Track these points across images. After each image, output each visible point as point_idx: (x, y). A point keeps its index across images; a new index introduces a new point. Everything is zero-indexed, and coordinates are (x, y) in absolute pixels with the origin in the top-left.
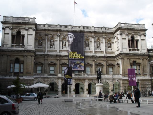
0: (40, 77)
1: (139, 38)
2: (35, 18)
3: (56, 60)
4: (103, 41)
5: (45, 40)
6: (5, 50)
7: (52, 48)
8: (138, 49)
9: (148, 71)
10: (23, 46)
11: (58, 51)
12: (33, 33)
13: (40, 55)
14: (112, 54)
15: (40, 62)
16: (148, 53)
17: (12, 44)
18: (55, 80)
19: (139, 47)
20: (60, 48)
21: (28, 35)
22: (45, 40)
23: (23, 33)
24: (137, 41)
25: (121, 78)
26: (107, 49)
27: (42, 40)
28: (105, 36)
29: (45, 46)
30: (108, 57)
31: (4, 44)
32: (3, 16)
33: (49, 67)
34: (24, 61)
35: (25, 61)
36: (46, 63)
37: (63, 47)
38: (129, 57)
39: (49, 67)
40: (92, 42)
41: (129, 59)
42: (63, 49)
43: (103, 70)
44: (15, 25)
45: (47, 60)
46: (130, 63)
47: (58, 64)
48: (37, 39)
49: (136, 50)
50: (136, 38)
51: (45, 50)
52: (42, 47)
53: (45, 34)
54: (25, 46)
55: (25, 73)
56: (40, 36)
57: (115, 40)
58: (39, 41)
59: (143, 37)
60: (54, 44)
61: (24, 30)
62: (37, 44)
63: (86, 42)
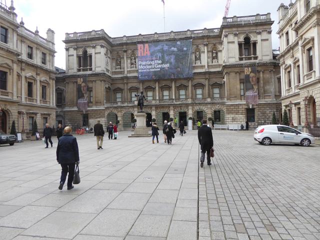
1: (258, 38)
2: (102, 30)
4: (204, 49)
6: (70, 76)
7: (133, 67)
9: (272, 90)
10: (91, 69)
12: (103, 51)
15: (118, 88)
18: (130, 109)
19: (258, 53)
21: (95, 53)
24: (255, 44)
27: (121, 58)
28: (208, 42)
30: (210, 73)
32: (66, 34)
34: (92, 88)
36: (126, 88)
38: (239, 71)
39: (131, 93)
41: (238, 74)
43: (204, 92)
44: (79, 44)
45: (127, 83)
50: (253, 38)
52: (121, 68)
54: (93, 69)
55: (94, 102)
56: (118, 53)
57: (223, 46)
58: (117, 60)
59: (265, 35)
62: (114, 64)
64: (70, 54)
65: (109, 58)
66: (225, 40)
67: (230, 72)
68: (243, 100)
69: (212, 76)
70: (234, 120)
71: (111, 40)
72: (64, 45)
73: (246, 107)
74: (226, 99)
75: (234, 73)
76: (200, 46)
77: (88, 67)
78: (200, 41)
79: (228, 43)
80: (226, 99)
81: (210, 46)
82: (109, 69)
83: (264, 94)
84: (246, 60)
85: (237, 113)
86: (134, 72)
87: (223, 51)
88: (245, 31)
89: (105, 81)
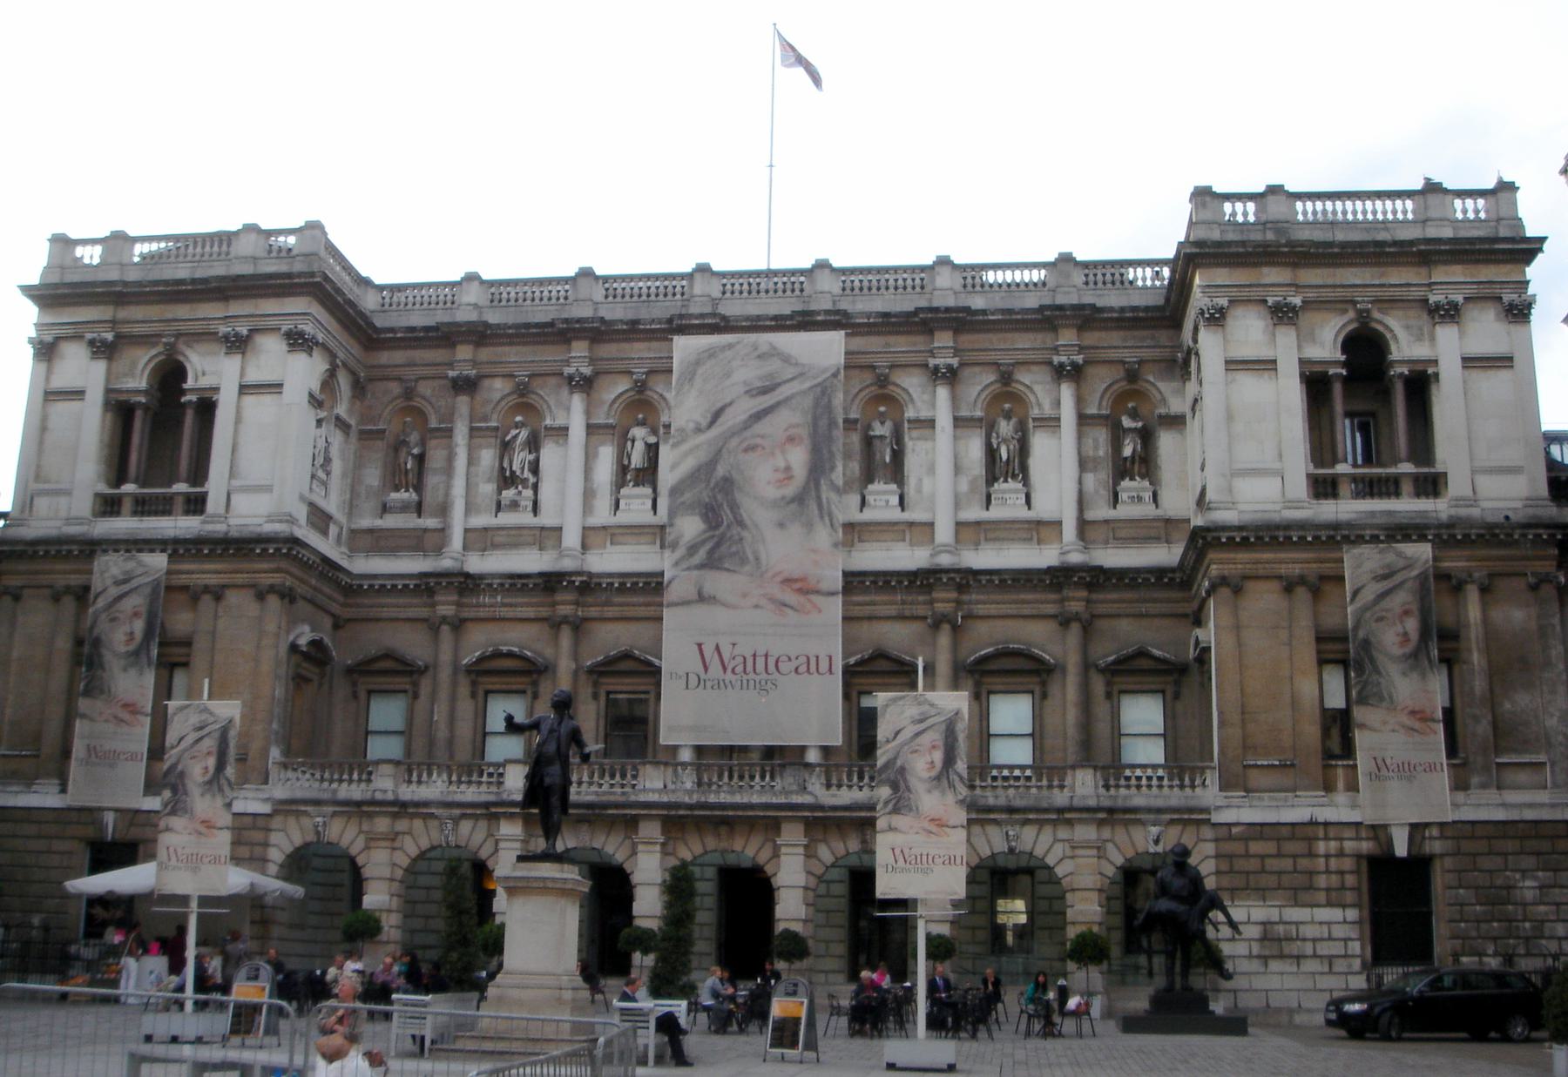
0: (326, 796)
2: (314, 227)
3: (546, 627)
4: (1058, 403)
5: (448, 433)
7: (514, 505)
8: (1439, 468)
9: (1552, 722)
10: (196, 504)
11: (571, 538)
12: (304, 372)
13: (388, 583)
14: (1157, 539)
15: (388, 655)
16: (1552, 512)
17: (104, 488)
18: (466, 826)
19: (1449, 452)
20: (587, 507)
21: (244, 389)
22: (451, 430)
23: (205, 382)
24: (1420, 384)
25: (1206, 810)
26: (1105, 494)
27: (427, 434)
28: (1081, 349)
29: (448, 487)
30: (1097, 578)
31: (41, 486)
33: (473, 695)
35: (201, 644)
36: (446, 656)
37: (624, 491)
39: (481, 698)
40: (930, 423)
41: (1302, 593)
42: (623, 518)
43: (1052, 721)
45: (458, 625)
46: (1319, 639)
47: (565, 666)
48: (383, 431)
49: (1407, 487)
51: (443, 532)
52: (419, 509)
53: (451, 374)
54: (214, 504)
56: (409, 393)
57: (1191, 388)
58: (399, 445)
60: (535, 468)
61: (214, 347)
62: (373, 476)
63: (869, 427)
64: (58, 383)
65: (341, 424)
66: (1211, 349)
67: (1246, 578)
68: (1341, 797)
69: (1108, 600)
70: (1275, 943)
71: (369, 302)
72: (29, 315)
73: (1366, 846)
74: (1212, 778)
75: (1275, 586)
76: (1024, 377)
77: (181, 487)
78: (1025, 342)
79: (1234, 365)
80: (1212, 778)
81: (1101, 381)
82: (332, 505)
83: (1498, 751)
84: (1358, 495)
85: (1299, 891)
86: (515, 538)
87: (1193, 426)
88: (1348, 294)
89: (288, 596)
